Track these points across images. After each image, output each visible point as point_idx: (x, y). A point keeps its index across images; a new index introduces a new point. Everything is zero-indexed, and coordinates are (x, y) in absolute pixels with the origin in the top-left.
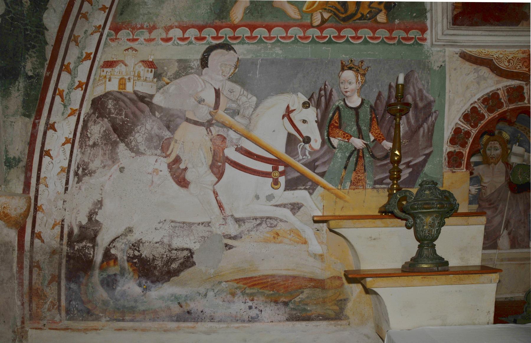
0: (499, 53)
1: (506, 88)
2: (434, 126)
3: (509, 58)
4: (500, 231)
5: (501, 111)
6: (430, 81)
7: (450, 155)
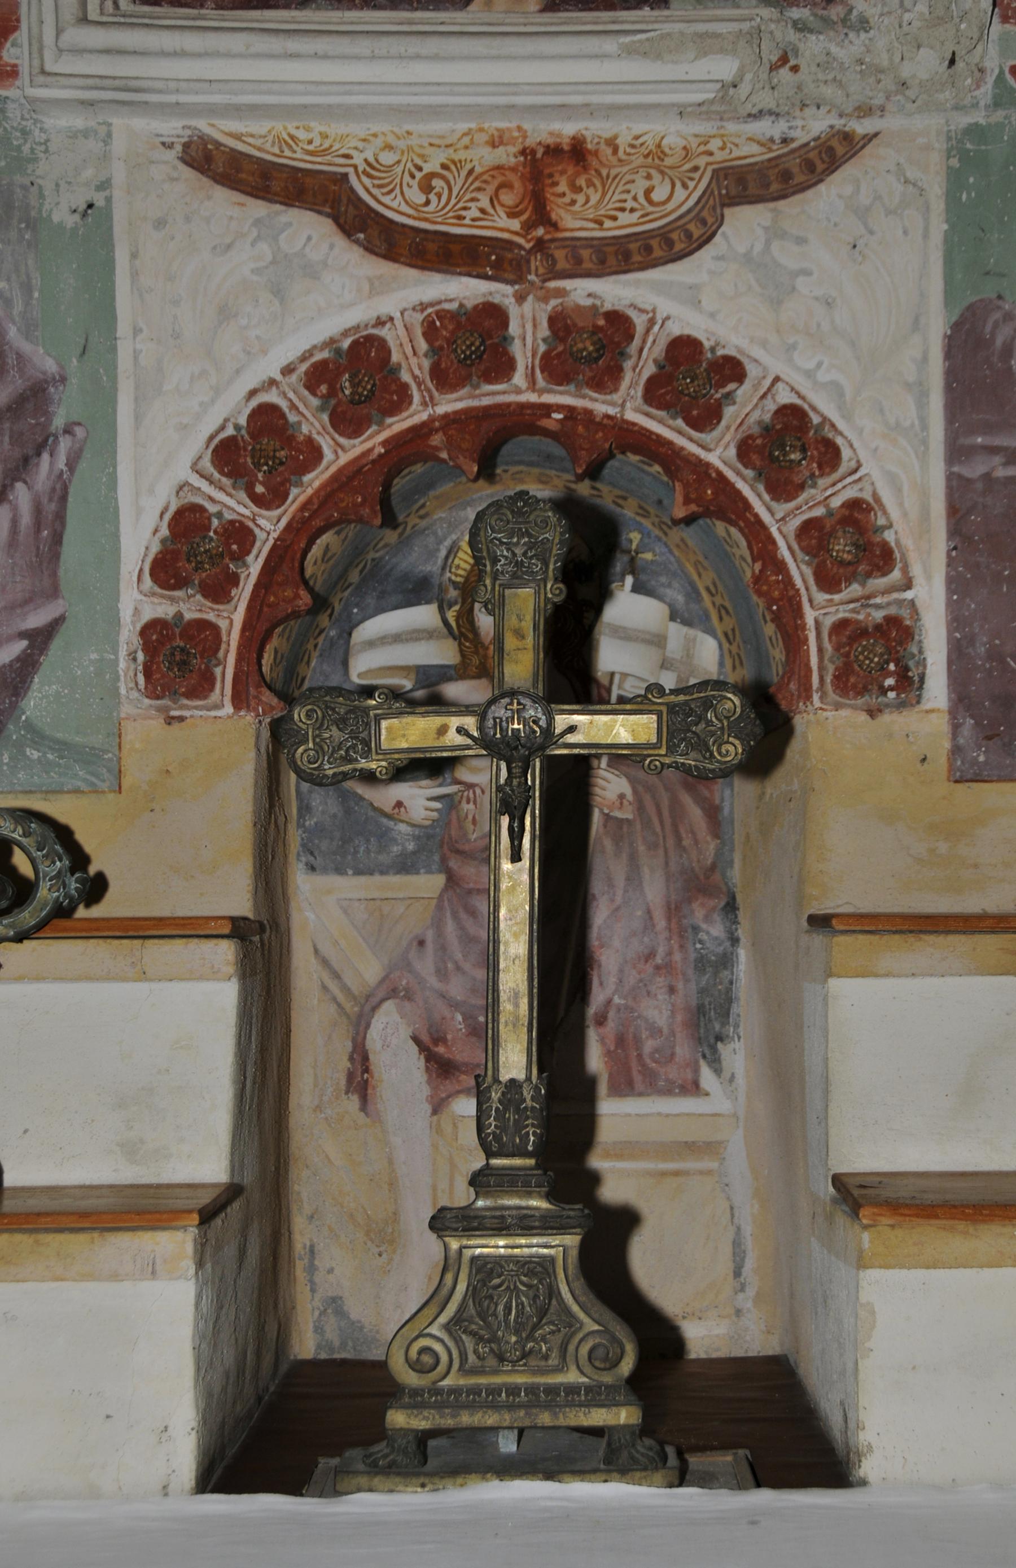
0: (379, 142)
1: (420, 317)
2: (64, 499)
3: (427, 168)
5: (398, 424)
6: (37, 281)
7: (155, 635)
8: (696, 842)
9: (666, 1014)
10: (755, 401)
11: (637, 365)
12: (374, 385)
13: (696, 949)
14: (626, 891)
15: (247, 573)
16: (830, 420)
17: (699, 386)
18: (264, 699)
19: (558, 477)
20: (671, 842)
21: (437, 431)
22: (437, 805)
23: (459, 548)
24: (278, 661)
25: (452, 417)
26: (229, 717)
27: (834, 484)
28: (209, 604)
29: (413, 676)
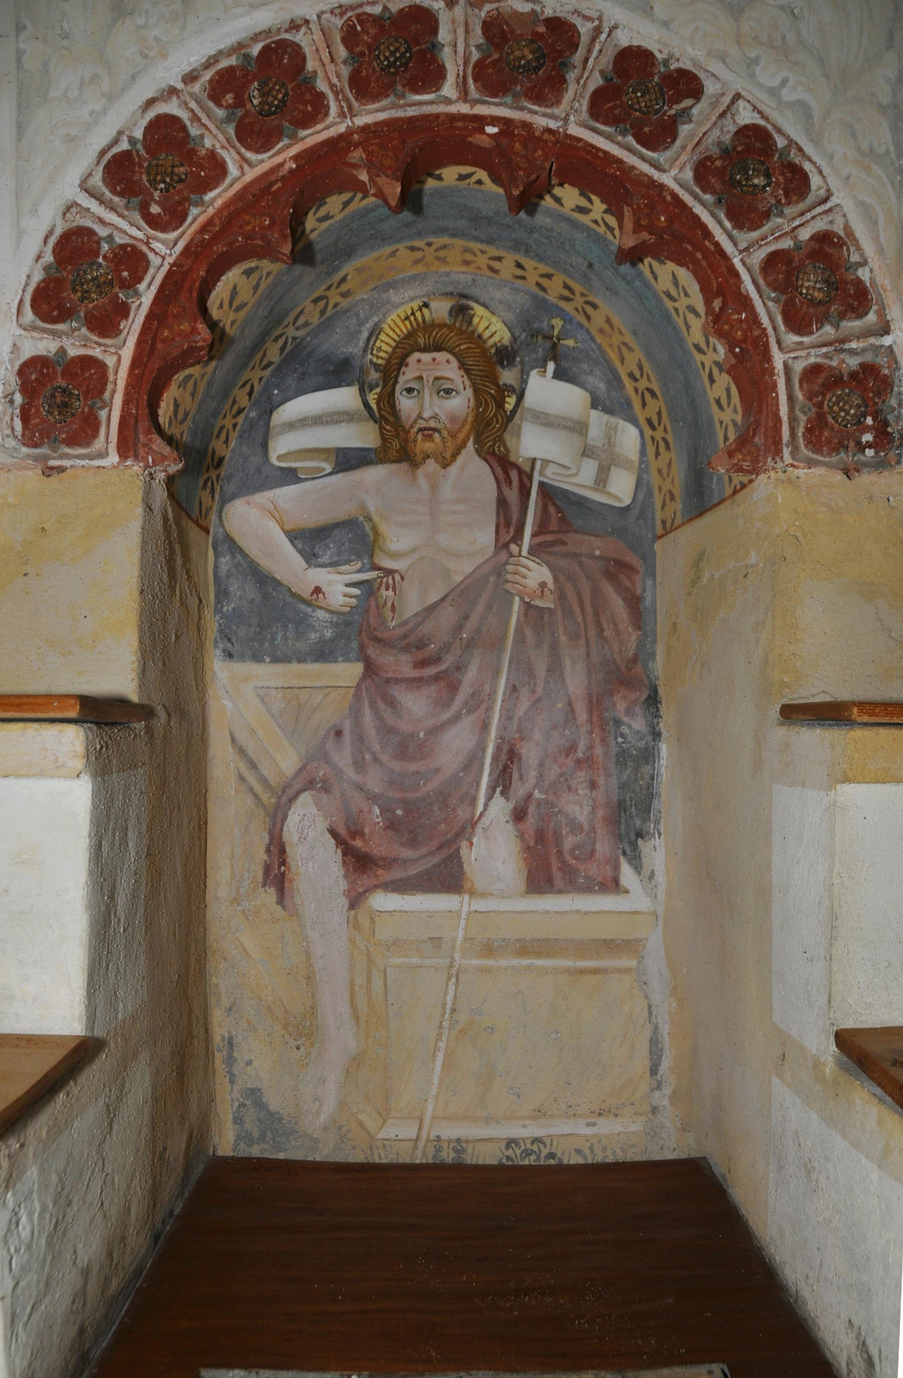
1: (339, 22)
4: (474, 800)
5: (312, 137)
8: (618, 633)
9: (587, 809)
10: (714, 119)
11: (582, 77)
12: (286, 95)
13: (617, 743)
14: (547, 682)
15: (137, 303)
16: (796, 143)
17: (651, 100)
18: (154, 447)
19: (483, 252)
20: (592, 632)
21: (356, 145)
22: (356, 591)
23: (381, 330)
24: (180, 417)
25: (373, 129)
26: (114, 467)
27: (802, 214)
28: (96, 338)
29: (333, 458)
